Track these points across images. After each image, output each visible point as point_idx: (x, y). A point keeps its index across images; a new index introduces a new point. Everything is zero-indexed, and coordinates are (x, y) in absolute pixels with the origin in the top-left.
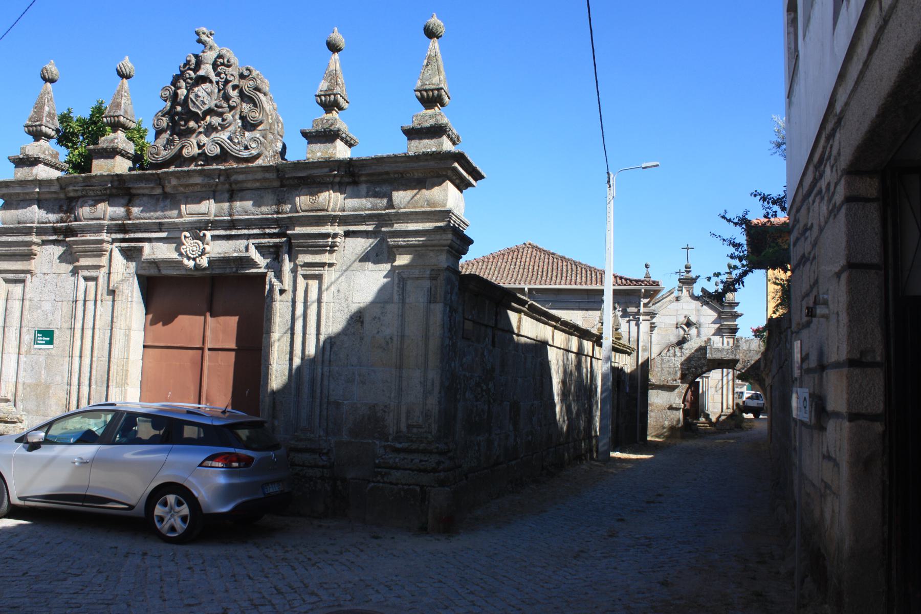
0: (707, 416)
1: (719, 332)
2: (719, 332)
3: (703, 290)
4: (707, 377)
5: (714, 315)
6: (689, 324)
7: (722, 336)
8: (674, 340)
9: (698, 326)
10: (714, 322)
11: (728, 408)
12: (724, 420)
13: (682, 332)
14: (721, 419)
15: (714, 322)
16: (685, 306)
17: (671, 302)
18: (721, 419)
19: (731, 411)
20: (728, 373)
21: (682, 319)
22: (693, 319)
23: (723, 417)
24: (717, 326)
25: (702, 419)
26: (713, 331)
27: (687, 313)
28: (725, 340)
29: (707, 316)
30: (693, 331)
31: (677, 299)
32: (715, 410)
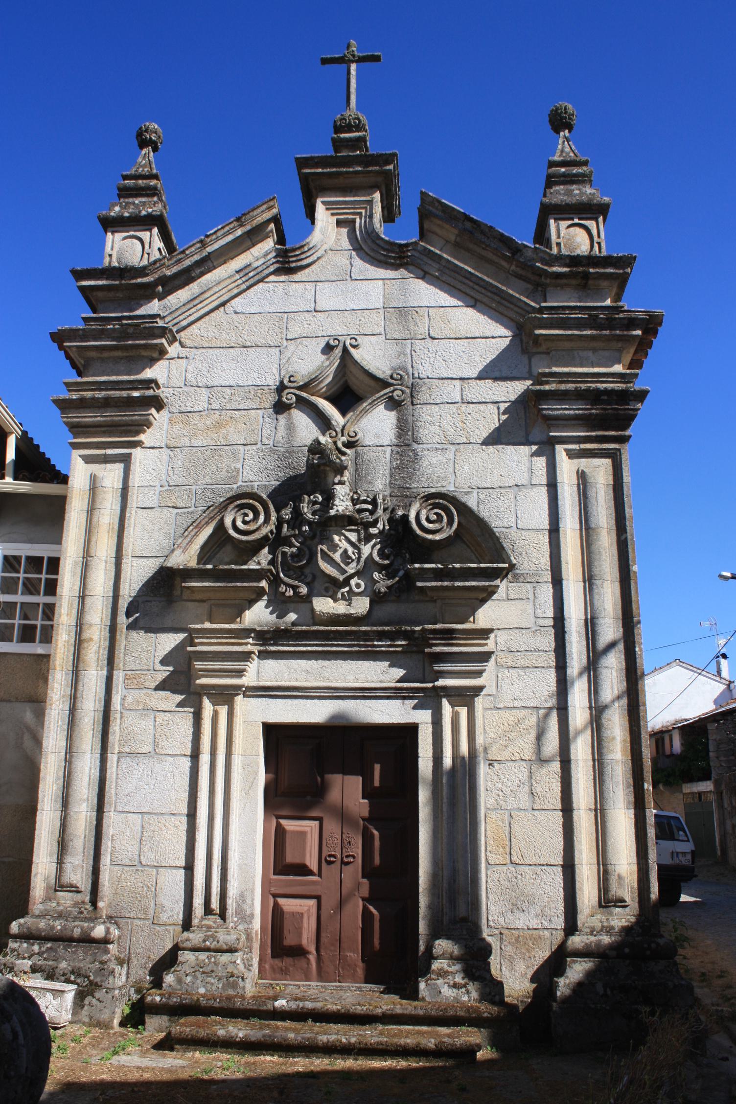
0: (476, 960)
1: (525, 424)
2: (525, 424)
3: (431, 212)
4: (466, 697)
5: (492, 336)
6: (351, 388)
7: (547, 448)
8: (258, 474)
9: (399, 393)
10: (494, 372)
11: (607, 901)
12: (579, 987)
13: (306, 430)
14: (564, 985)
15: (494, 372)
16: (328, 296)
17: (252, 279)
18: (564, 985)
19: (621, 918)
20: (592, 667)
21: (309, 362)
22: (374, 357)
23: (577, 971)
24: (513, 390)
25: (446, 986)
26: (490, 420)
27: (337, 327)
28: (567, 469)
29: (454, 344)
30: (376, 425)
31: (288, 263)
32: (523, 921)
